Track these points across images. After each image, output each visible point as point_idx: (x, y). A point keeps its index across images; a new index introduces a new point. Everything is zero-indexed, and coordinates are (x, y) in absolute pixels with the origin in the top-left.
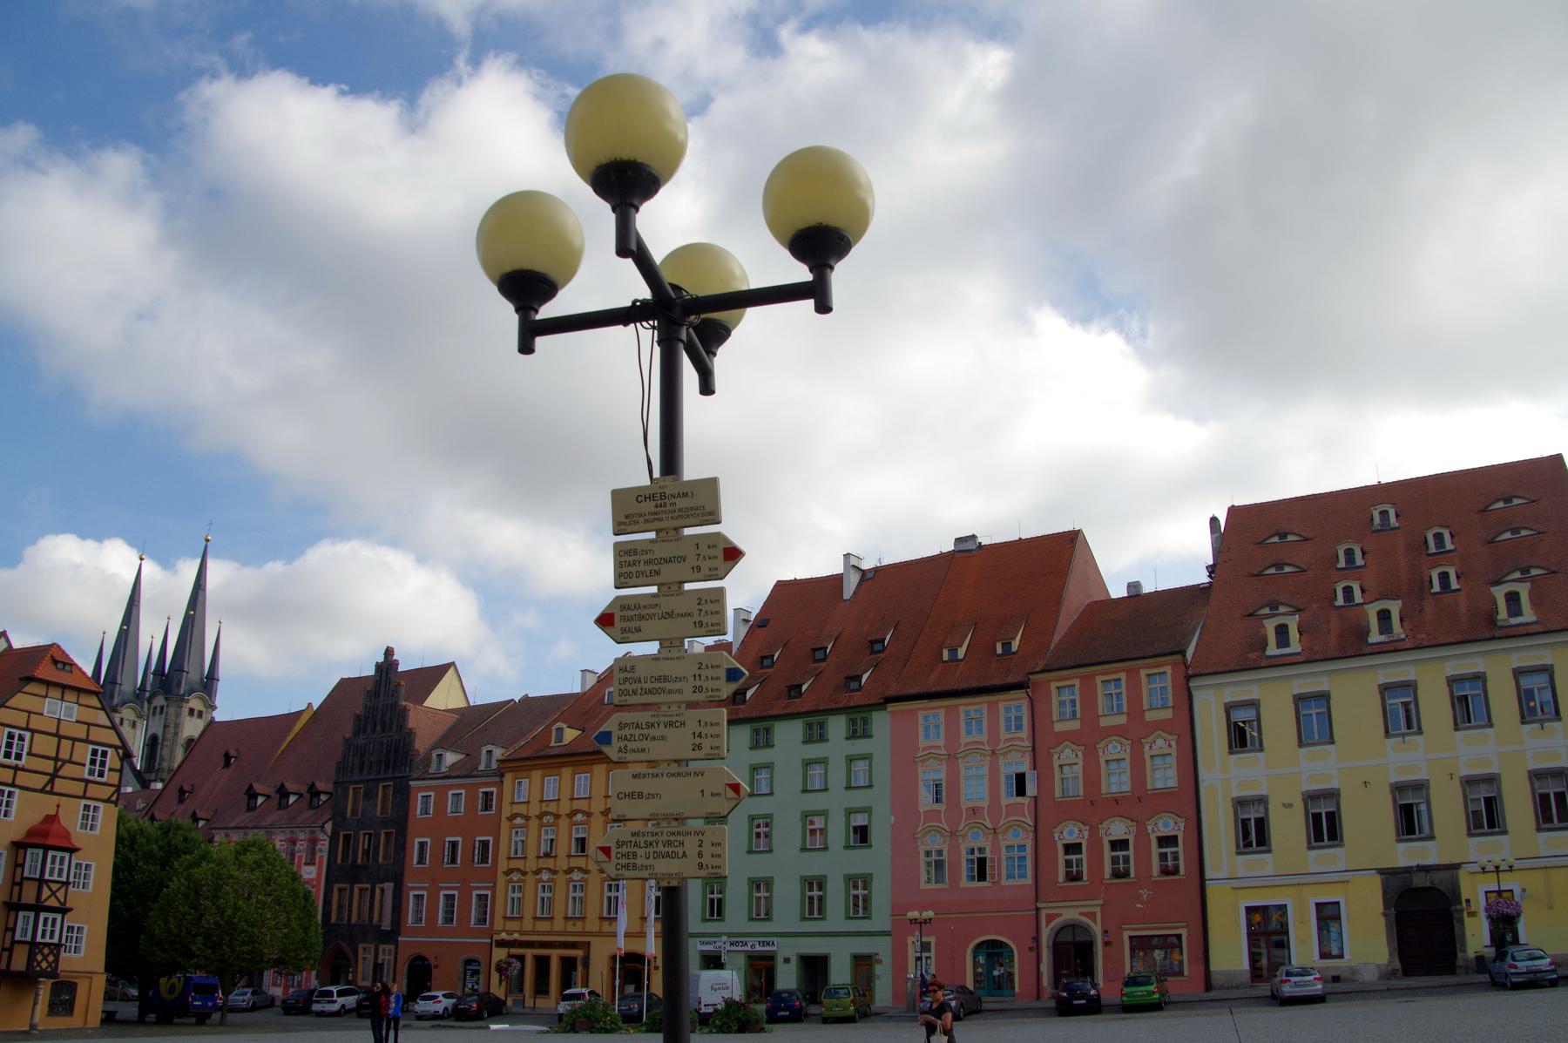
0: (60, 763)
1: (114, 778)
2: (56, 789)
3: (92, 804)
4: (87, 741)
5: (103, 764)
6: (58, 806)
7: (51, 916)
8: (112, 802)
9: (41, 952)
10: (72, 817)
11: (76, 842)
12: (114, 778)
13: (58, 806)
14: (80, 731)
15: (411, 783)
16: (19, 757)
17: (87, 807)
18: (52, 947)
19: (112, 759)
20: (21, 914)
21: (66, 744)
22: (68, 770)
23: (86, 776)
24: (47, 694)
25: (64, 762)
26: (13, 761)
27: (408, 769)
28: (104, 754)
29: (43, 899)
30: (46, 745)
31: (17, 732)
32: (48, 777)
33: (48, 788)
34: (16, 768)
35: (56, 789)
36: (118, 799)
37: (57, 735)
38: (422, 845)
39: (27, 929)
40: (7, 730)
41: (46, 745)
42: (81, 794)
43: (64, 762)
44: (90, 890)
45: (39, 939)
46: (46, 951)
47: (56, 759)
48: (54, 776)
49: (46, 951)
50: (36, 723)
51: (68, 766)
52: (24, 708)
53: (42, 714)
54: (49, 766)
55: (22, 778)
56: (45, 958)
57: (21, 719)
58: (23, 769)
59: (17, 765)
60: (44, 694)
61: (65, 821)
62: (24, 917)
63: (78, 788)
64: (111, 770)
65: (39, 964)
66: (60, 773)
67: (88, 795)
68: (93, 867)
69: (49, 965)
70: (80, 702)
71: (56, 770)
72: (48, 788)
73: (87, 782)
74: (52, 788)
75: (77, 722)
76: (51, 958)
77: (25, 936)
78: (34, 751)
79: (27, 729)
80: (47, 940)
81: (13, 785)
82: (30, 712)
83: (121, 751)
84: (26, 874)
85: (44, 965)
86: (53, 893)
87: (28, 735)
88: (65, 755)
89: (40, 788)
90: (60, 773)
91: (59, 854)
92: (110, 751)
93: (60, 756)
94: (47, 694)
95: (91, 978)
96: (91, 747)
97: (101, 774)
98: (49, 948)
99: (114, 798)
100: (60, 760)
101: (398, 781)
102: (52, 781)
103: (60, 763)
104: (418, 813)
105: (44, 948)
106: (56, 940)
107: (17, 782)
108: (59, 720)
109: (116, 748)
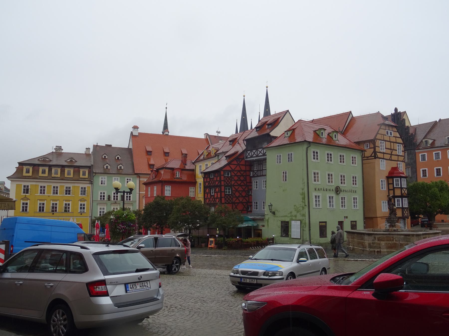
0: (392, 150)
2: (392, 159)
4: (396, 143)
15: (416, 151)
20: (396, 199)
22: (394, 153)
23: (398, 154)
27: (411, 146)
33: (391, 159)
34: (384, 153)
37: (390, 141)
38: (424, 171)
39: (399, 204)
42: (397, 160)
49: (406, 210)
52: (382, 134)
53: (386, 135)
56: (406, 212)
62: (397, 200)
65: (405, 214)
69: (407, 215)
70: (393, 130)
75: (394, 137)
77: (399, 206)
78: (386, 147)
79: (384, 140)
81: (383, 159)
83: (403, 145)
84: (395, 186)
85: (406, 214)
92: (401, 145)
96: (397, 144)
99: (404, 160)
101: (409, 151)
104: (420, 160)
108: (390, 136)
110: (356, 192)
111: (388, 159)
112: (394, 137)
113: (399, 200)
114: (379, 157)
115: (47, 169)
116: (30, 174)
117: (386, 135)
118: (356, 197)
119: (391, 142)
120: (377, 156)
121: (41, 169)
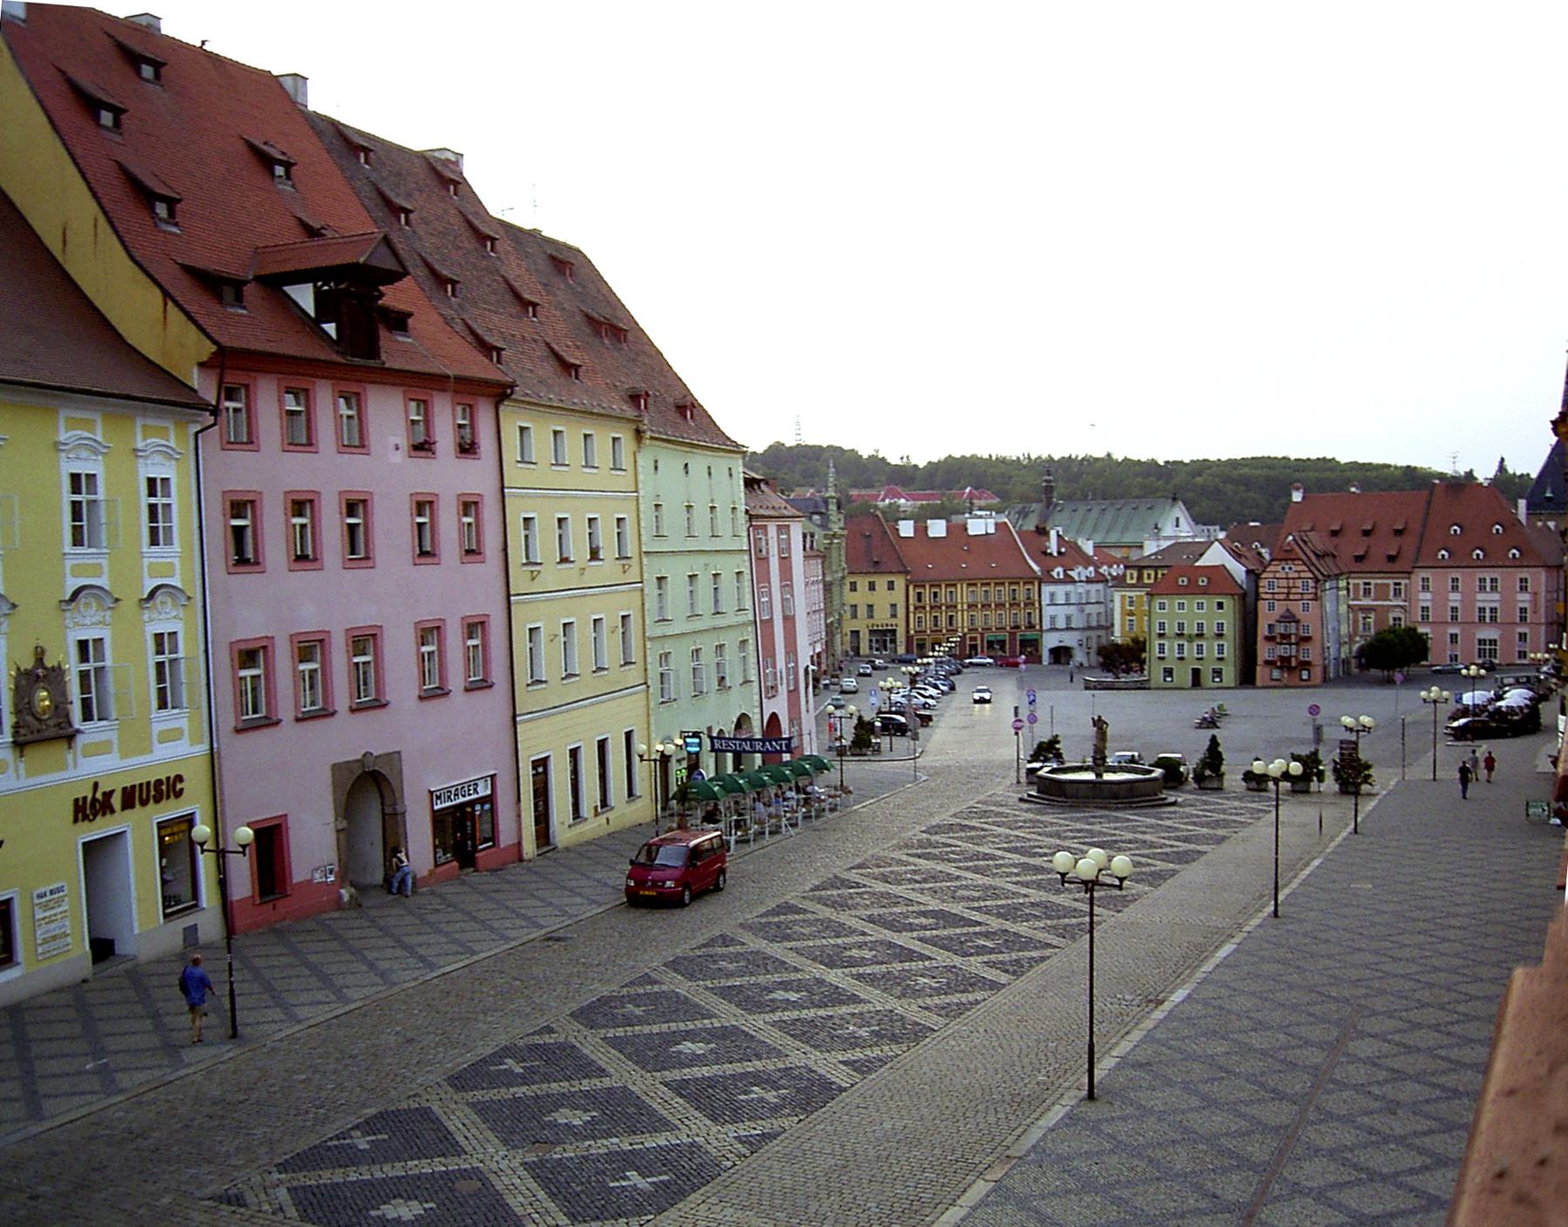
1: (1313, 590)
4: (1300, 578)
10: (1297, 608)
11: (1298, 617)
12: (1313, 590)
14: (1296, 575)
19: (1311, 583)
22: (1293, 590)
23: (1301, 591)
30: (1284, 583)
37: (1287, 578)
41: (1284, 583)
48: (1288, 594)
50: (1278, 575)
54: (1286, 591)
55: (1276, 596)
57: (1271, 575)
61: (1293, 610)
63: (1299, 597)
115: (1152, 573)
116: (1134, 581)
119: (1287, 578)
121: (1145, 573)
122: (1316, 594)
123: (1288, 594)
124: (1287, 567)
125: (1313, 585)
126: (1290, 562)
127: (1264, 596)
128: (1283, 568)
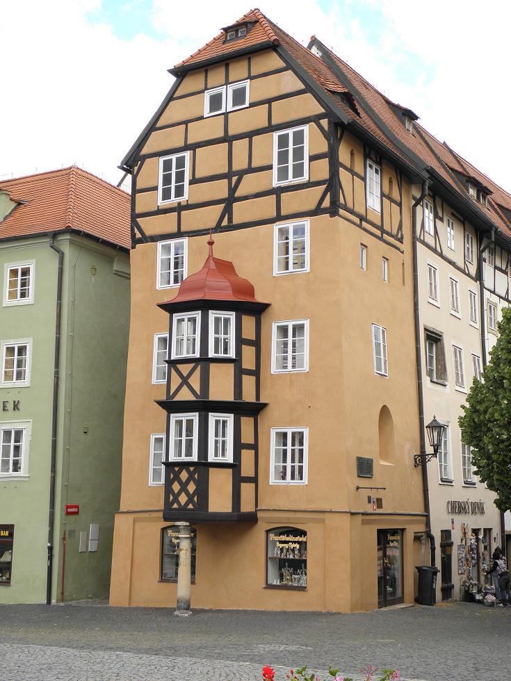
0: (235, 179)
2: (236, 221)
3: (290, 225)
4: (271, 128)
5: (299, 154)
6: (211, 243)
7: (184, 417)
8: (325, 211)
9: (177, 478)
13: (211, 243)
14: (258, 118)
16: (179, 191)
17: (284, 233)
18: (192, 469)
21: (240, 146)
22: (249, 185)
23: (276, 183)
24: (206, 84)
25: (241, 174)
26: (173, 201)
28: (299, 137)
29: (172, 392)
31: (174, 157)
32: (223, 205)
33: (225, 223)
34: (180, 208)
35: (236, 221)
36: (335, 202)
37: (228, 139)
40: (162, 160)
41: (212, 160)
43: (241, 174)
44: (306, 368)
45: (172, 459)
46: (184, 475)
47: (227, 176)
48: (229, 202)
49: (184, 475)
50: (198, 133)
51: (247, 178)
53: (202, 118)
54: (220, 189)
55: (192, 220)
56: (184, 487)
57: (174, 138)
58: (189, 207)
59: (179, 204)
60: (203, 87)
63: (266, 207)
64: (312, 158)
65: (176, 500)
66: (237, 194)
67: (283, 213)
68: (307, 328)
71: (232, 190)
72: (225, 223)
73: (278, 192)
74: (230, 220)
75: (252, 105)
76: (192, 488)
78: (197, 176)
79: (186, 147)
80: (184, 458)
81: (179, 234)
82: (186, 123)
83: (324, 122)
85: (183, 499)
86: (185, 381)
87: (187, 155)
88: (240, 163)
89: (214, 225)
90: (237, 194)
91: (186, 315)
92: (306, 128)
93: (235, 167)
94: (206, 84)
95: (323, 521)
96: (276, 135)
97: (298, 171)
98: (188, 471)
99: (326, 203)
100: (235, 174)
102: (228, 211)
103: (235, 179)
105: (180, 472)
106: (195, 458)
107: (183, 229)
108: (226, 114)
109: (316, 119)
110: (16, 407)
111: (209, 229)
112: (252, 105)
113: (224, 422)
114: (148, 232)
117: (202, 118)
118: (19, 427)
120: (138, 235)
122: (333, 185)
123: (229, 202)
124: (228, 93)
125: (323, 147)
126: (238, 70)
127: (151, 226)
128: (216, 102)
